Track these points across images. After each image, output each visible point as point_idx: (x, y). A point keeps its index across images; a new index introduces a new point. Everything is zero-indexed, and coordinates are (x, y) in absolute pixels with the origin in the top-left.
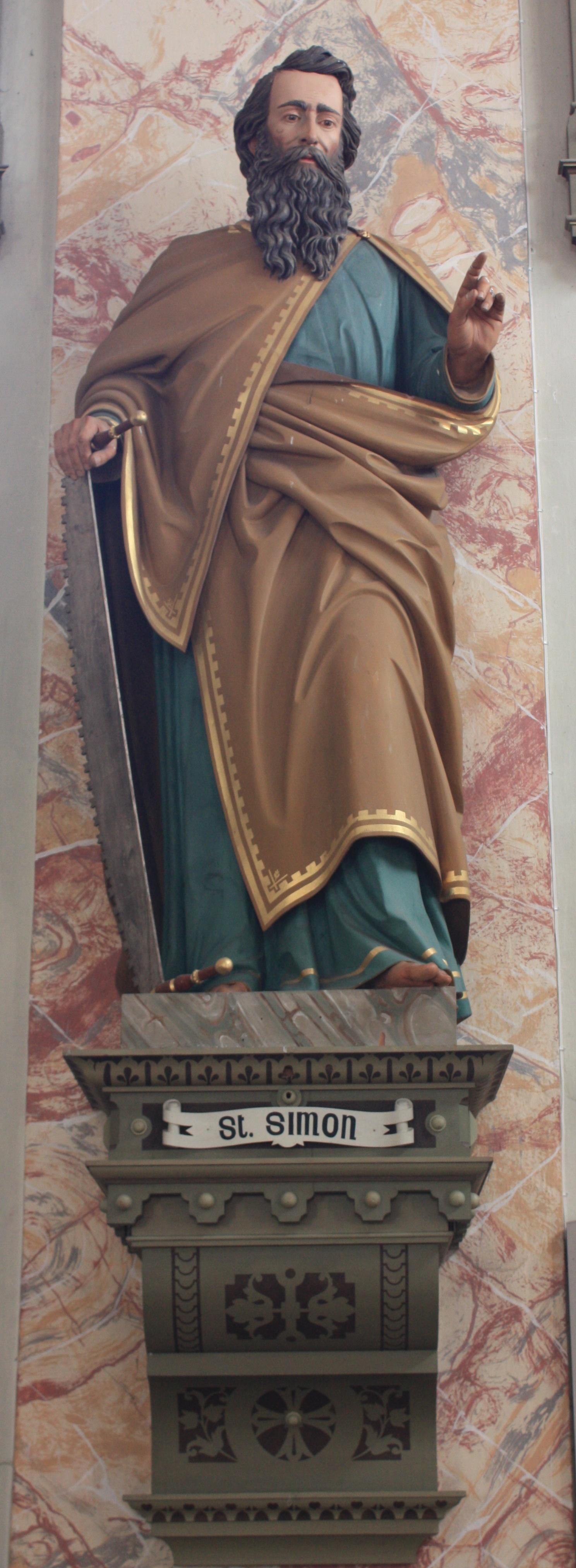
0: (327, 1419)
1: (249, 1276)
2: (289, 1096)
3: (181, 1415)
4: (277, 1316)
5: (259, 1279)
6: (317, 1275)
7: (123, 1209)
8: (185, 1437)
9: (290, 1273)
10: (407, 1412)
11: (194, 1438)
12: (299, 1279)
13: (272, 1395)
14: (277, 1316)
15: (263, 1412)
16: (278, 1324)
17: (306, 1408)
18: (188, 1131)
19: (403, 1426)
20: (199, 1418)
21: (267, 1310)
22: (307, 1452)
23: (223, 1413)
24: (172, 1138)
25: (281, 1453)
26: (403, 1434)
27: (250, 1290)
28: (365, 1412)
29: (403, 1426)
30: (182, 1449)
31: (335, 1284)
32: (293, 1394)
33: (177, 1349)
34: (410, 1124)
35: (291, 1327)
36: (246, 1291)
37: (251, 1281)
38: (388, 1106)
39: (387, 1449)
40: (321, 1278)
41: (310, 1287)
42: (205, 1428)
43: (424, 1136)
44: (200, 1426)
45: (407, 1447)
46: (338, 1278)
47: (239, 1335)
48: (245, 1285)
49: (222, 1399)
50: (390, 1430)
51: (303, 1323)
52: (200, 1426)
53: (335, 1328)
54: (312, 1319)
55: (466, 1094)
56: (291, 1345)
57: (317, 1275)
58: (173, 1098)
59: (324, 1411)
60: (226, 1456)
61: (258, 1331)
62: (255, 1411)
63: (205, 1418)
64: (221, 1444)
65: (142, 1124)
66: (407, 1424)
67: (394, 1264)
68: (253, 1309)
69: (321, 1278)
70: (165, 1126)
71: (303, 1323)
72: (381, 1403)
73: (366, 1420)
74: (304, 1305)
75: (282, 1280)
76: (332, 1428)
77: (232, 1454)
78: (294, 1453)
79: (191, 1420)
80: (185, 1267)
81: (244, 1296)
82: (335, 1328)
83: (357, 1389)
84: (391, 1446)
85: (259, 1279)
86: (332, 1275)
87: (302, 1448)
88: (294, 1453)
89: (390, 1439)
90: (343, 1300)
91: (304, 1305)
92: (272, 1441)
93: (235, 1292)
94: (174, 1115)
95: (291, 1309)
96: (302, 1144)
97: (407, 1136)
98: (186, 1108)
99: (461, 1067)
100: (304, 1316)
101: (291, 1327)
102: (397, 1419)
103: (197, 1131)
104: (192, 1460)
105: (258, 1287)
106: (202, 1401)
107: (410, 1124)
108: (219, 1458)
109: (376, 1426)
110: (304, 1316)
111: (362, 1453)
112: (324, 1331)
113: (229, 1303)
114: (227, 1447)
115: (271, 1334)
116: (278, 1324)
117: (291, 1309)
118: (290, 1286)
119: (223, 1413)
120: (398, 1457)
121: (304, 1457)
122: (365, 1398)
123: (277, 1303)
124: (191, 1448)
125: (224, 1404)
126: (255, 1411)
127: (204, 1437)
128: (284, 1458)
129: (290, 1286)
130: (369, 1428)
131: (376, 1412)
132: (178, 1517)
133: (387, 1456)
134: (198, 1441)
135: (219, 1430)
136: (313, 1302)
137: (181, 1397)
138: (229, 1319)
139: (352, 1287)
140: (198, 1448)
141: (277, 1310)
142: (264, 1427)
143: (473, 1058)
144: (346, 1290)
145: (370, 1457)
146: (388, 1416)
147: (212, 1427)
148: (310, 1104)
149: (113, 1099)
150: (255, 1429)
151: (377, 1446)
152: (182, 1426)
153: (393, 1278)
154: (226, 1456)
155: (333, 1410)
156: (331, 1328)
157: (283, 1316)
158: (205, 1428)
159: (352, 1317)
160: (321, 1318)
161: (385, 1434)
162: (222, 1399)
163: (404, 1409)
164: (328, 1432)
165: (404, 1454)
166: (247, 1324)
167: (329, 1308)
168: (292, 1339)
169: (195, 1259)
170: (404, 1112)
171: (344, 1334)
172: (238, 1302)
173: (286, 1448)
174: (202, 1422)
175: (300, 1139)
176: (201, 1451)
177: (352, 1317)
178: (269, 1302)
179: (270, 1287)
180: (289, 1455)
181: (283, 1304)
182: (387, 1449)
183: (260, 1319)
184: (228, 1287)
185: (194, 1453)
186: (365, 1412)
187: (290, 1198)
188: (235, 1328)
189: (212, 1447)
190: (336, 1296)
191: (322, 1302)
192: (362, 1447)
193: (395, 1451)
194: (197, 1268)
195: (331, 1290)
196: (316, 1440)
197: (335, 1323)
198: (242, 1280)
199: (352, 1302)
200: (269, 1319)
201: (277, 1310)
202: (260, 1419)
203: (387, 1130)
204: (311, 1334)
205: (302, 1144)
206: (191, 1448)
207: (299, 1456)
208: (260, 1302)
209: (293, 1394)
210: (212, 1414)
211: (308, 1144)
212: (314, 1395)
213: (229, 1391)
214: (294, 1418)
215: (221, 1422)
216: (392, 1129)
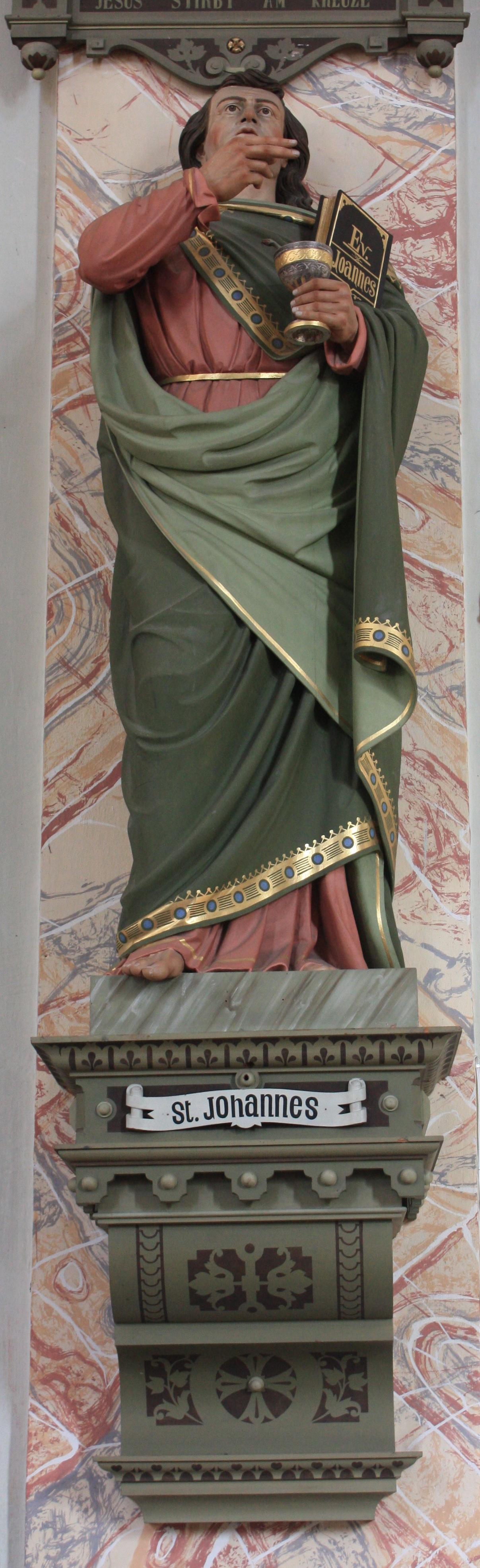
0: (289, 1383)
1: (210, 1252)
2: (246, 1078)
3: (148, 1380)
4: (238, 1288)
5: (220, 1254)
6: (276, 1249)
7: (88, 1190)
8: (153, 1401)
9: (250, 1249)
10: (365, 1377)
11: (161, 1402)
12: (258, 1254)
13: (236, 1361)
14: (238, 1288)
15: (227, 1377)
16: (239, 1296)
17: (267, 1373)
18: (150, 1114)
19: (361, 1390)
20: (166, 1383)
21: (228, 1283)
22: (270, 1416)
23: (188, 1379)
24: (134, 1121)
25: (243, 1417)
26: (361, 1398)
27: (211, 1265)
28: (324, 1378)
29: (361, 1390)
30: (150, 1413)
31: (292, 1258)
32: (255, 1359)
33: (144, 1319)
34: (364, 1104)
35: (252, 1299)
36: (207, 1266)
37: (212, 1257)
38: (343, 1087)
39: (347, 1412)
40: (280, 1253)
41: (270, 1259)
42: (171, 1393)
43: (376, 1116)
44: (166, 1390)
45: (365, 1409)
46: (296, 1253)
47: (202, 1308)
48: (207, 1260)
49: (187, 1366)
50: (350, 1394)
51: (264, 1296)
52: (166, 1390)
53: (294, 1299)
54: (272, 1291)
55: (418, 1075)
56: (252, 1317)
57: (276, 1249)
58: (134, 1083)
59: (285, 1376)
60: (192, 1418)
61: (219, 1303)
62: (218, 1376)
63: (171, 1383)
64: (186, 1407)
65: (106, 1106)
66: (365, 1388)
67: (349, 1238)
68: (214, 1282)
69: (280, 1253)
70: (128, 1110)
71: (264, 1296)
72: (340, 1369)
73: (326, 1385)
74: (263, 1278)
75: (242, 1254)
76: (293, 1392)
77: (198, 1418)
78: (257, 1416)
79: (157, 1386)
80: (150, 1243)
81: (207, 1271)
82: (294, 1299)
83: (317, 1356)
84: (350, 1409)
85: (220, 1254)
86: (289, 1249)
87: (265, 1411)
88: (257, 1416)
89: (349, 1403)
90: (300, 1273)
91: (263, 1278)
92: (235, 1405)
93: (196, 1266)
94: (135, 1097)
95: (251, 1282)
96: (260, 1125)
97: (359, 1115)
98: (148, 1092)
99: (412, 1049)
100: (264, 1288)
101: (252, 1299)
102: (356, 1382)
103: (154, 1114)
104: (159, 1423)
105: (219, 1261)
106: (168, 1368)
107: (364, 1104)
108: (185, 1421)
109: (335, 1390)
110: (264, 1288)
111: (322, 1416)
112: (284, 1303)
113: (191, 1277)
114: (192, 1411)
115: (232, 1307)
116: (239, 1296)
117: (251, 1282)
118: (250, 1261)
119: (188, 1379)
120: (357, 1420)
121: (266, 1420)
122: (324, 1363)
123: (237, 1278)
124: (159, 1412)
125: (189, 1370)
126: (218, 1376)
127: (170, 1401)
128: (247, 1420)
129: (250, 1261)
130: (329, 1393)
131: (335, 1376)
132: (147, 1477)
133: (347, 1418)
134: (165, 1405)
135: (185, 1394)
136: (272, 1274)
137: (147, 1364)
138: (192, 1291)
139: (309, 1260)
140: (165, 1412)
141: (238, 1284)
142: (227, 1392)
143: (423, 1041)
144: (303, 1263)
145: (329, 1419)
146: (347, 1380)
147: (178, 1392)
148: (267, 1086)
149: (78, 1082)
150: (219, 1393)
151: (337, 1407)
152: (149, 1391)
153: (349, 1250)
154: (192, 1418)
155: (293, 1375)
156: (290, 1299)
157: (244, 1289)
158: (171, 1393)
159: (310, 1289)
160: (280, 1290)
161: (344, 1398)
162: (187, 1366)
163: (362, 1374)
164: (289, 1395)
165: (363, 1416)
166: (209, 1296)
167: (287, 1280)
168: (252, 1310)
169: (158, 1235)
170: (357, 1091)
171: (302, 1306)
172: (200, 1275)
173: (249, 1412)
174: (168, 1388)
175: (258, 1121)
176: (168, 1415)
177: (310, 1289)
178: (229, 1276)
179: (230, 1260)
180: (252, 1418)
181: (243, 1277)
182: (347, 1412)
183: (222, 1291)
184: (190, 1263)
185: (161, 1417)
186: (324, 1378)
187: (249, 1177)
188: (198, 1300)
189: (179, 1410)
190: (293, 1269)
191: (280, 1275)
192: (322, 1409)
193: (353, 1413)
194: (161, 1243)
195: (289, 1263)
196: (277, 1403)
197: (293, 1294)
198: (204, 1255)
199: (309, 1275)
200: (230, 1291)
201: (238, 1284)
202: (224, 1384)
203: (342, 1109)
204: (271, 1306)
205: (260, 1125)
206: (159, 1412)
207: (261, 1418)
208: (222, 1276)
209: (255, 1359)
210: (178, 1379)
211: (265, 1125)
212: (275, 1360)
213: (194, 1358)
214: (257, 1383)
215: (187, 1387)
216: (346, 1108)
